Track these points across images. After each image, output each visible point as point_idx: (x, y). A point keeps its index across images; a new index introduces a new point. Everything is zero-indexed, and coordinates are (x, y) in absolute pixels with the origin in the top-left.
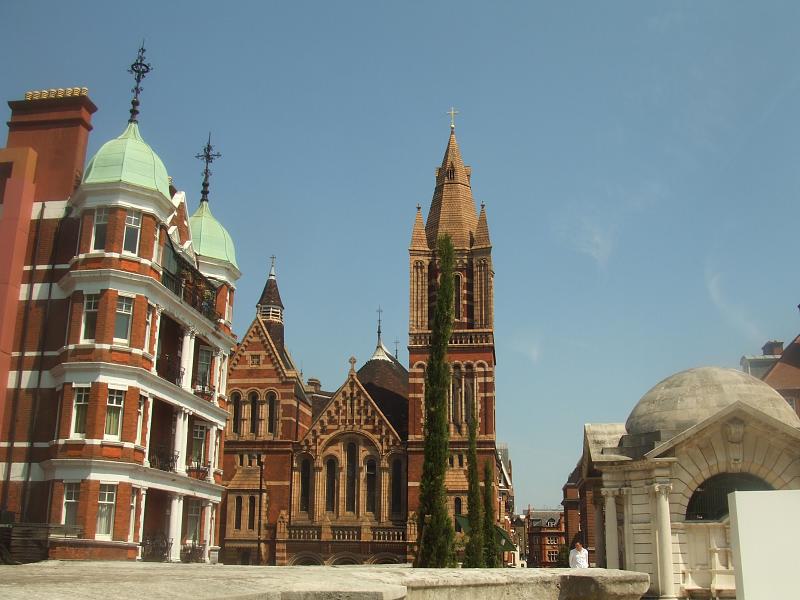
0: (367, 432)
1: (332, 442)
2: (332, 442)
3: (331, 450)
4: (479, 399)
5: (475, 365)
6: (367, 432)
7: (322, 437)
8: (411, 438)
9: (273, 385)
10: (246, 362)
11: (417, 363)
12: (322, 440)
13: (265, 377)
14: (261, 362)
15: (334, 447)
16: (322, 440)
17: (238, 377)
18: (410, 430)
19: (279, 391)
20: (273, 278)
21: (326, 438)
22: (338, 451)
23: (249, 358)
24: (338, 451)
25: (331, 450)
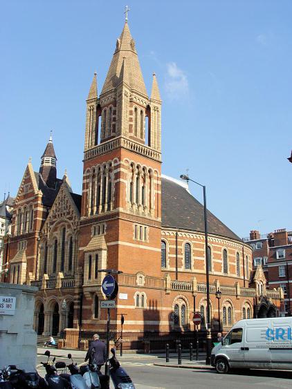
1: (55, 229)
6: (68, 220)
15: (56, 232)
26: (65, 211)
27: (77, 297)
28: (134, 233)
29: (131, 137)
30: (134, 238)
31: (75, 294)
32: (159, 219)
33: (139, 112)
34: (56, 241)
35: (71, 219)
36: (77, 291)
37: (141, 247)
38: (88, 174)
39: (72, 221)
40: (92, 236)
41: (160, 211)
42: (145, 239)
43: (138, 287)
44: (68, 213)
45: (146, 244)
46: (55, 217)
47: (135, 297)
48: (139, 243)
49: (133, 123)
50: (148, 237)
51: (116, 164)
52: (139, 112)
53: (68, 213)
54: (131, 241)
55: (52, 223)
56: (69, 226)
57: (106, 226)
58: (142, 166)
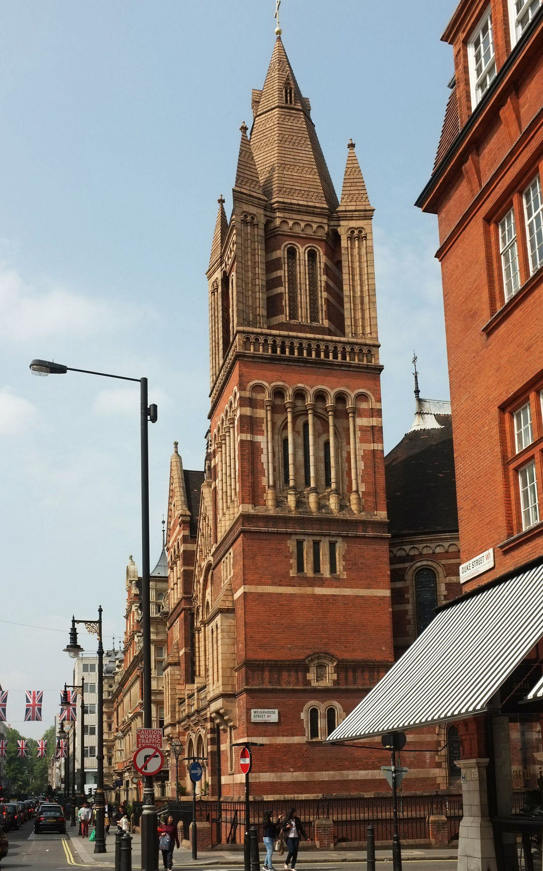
28: (293, 561)
29: (280, 326)
30: (293, 573)
32: (382, 515)
33: (302, 252)
37: (319, 591)
41: (382, 495)
42: (333, 569)
43: (315, 691)
45: (335, 581)
47: (304, 716)
48: (322, 582)
49: (284, 289)
50: (340, 566)
52: (302, 252)
54: (291, 582)
58: (311, 392)
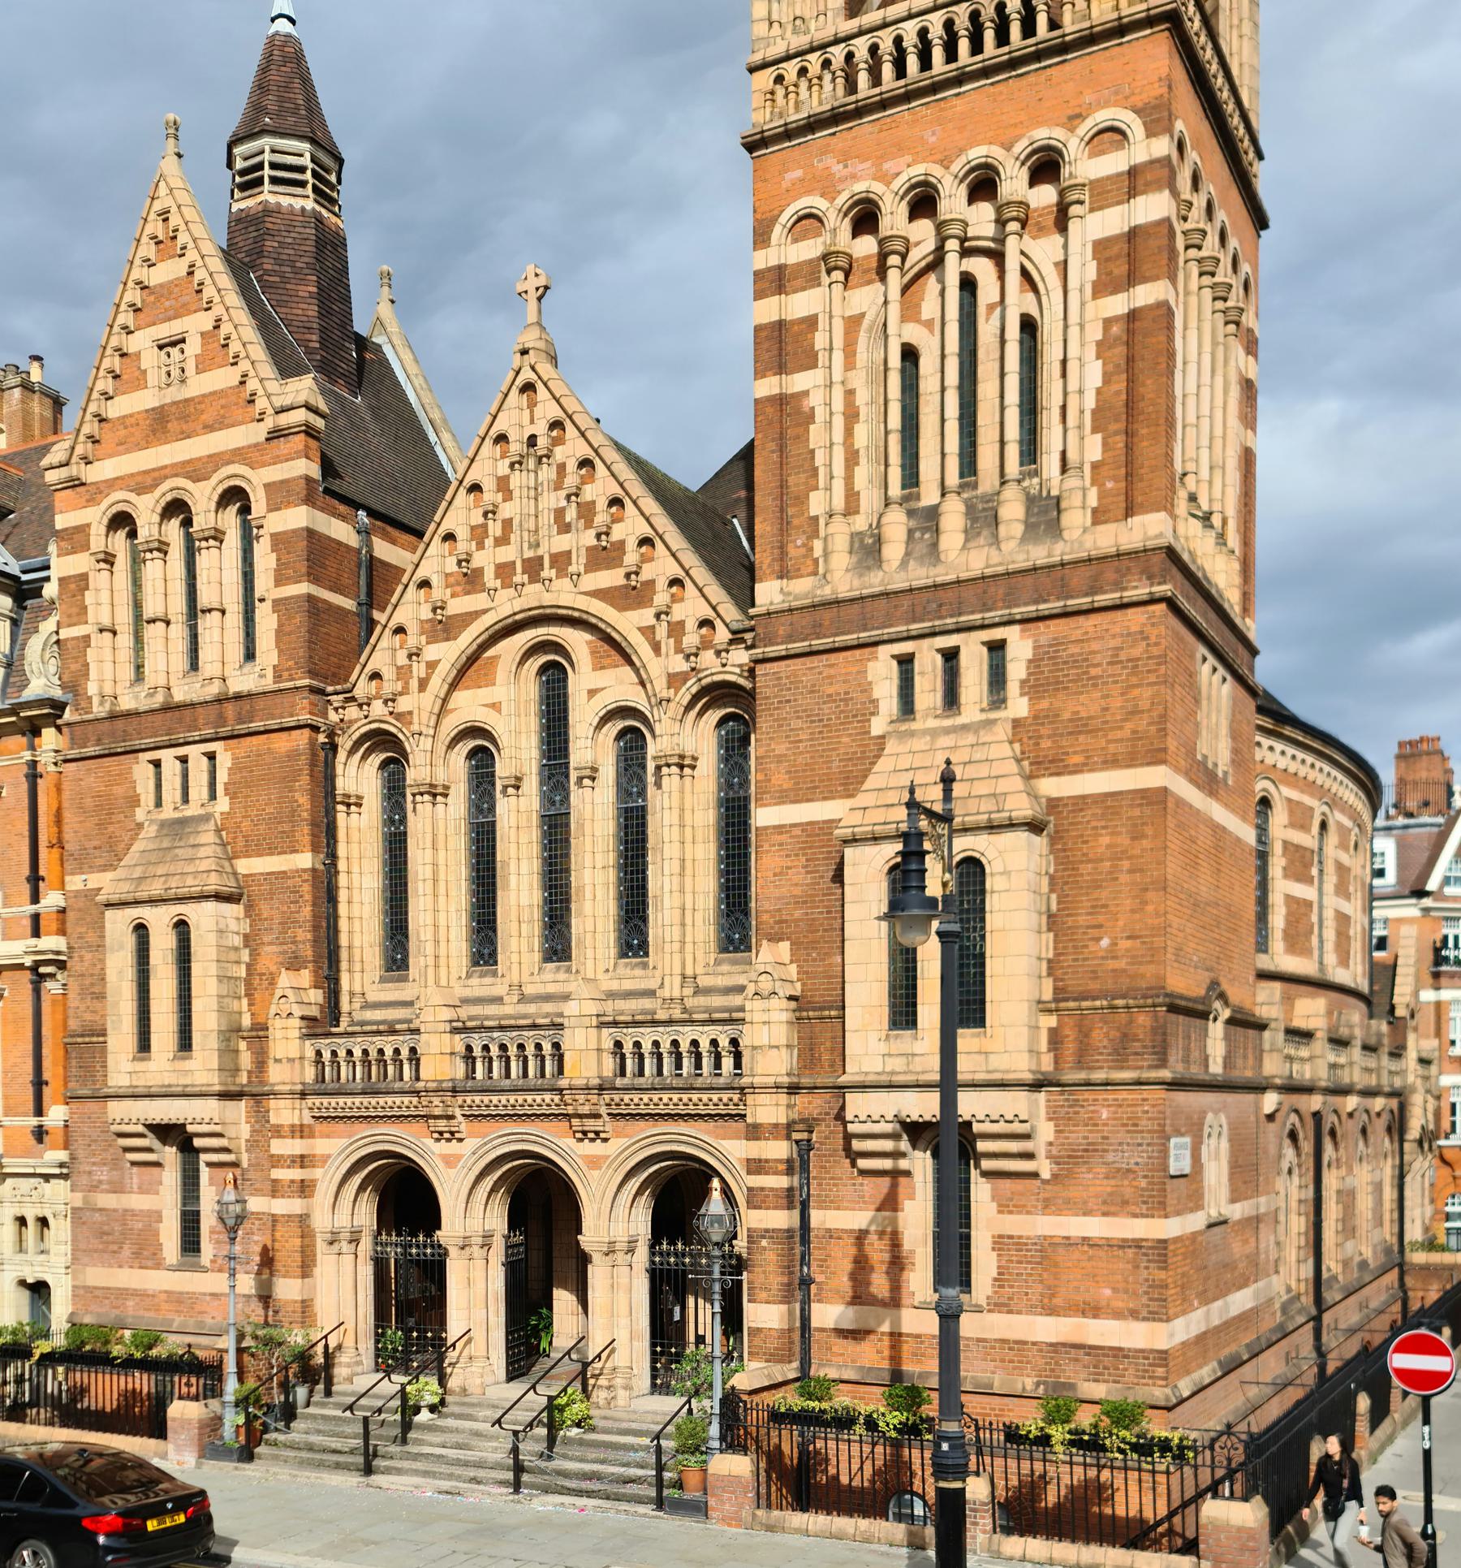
0: (599, 609)
1: (469, 668)
2: (469, 668)
3: (469, 706)
4: (1095, 333)
5: (1073, 148)
7: (432, 652)
8: (768, 593)
9: (238, 455)
10: (140, 382)
11: (787, 216)
12: (432, 665)
13: (209, 428)
14: (190, 367)
15: (485, 694)
16: (432, 665)
17: (125, 446)
18: (763, 558)
19: (256, 481)
20: (283, 26)
21: (448, 653)
22: (495, 706)
23: (151, 359)
24: (495, 706)
25: (469, 706)
26: (562, 543)
27: (779, 1150)
31: (755, 1132)
34: (482, 761)
35: (633, 594)
36: (768, 1110)
38: (809, 250)
39: (646, 616)
40: (878, 726)
44: (604, 555)
46: (471, 580)
51: (1114, 163)
53: (604, 555)
55: (443, 627)
56: (615, 647)
57: (1020, 647)
